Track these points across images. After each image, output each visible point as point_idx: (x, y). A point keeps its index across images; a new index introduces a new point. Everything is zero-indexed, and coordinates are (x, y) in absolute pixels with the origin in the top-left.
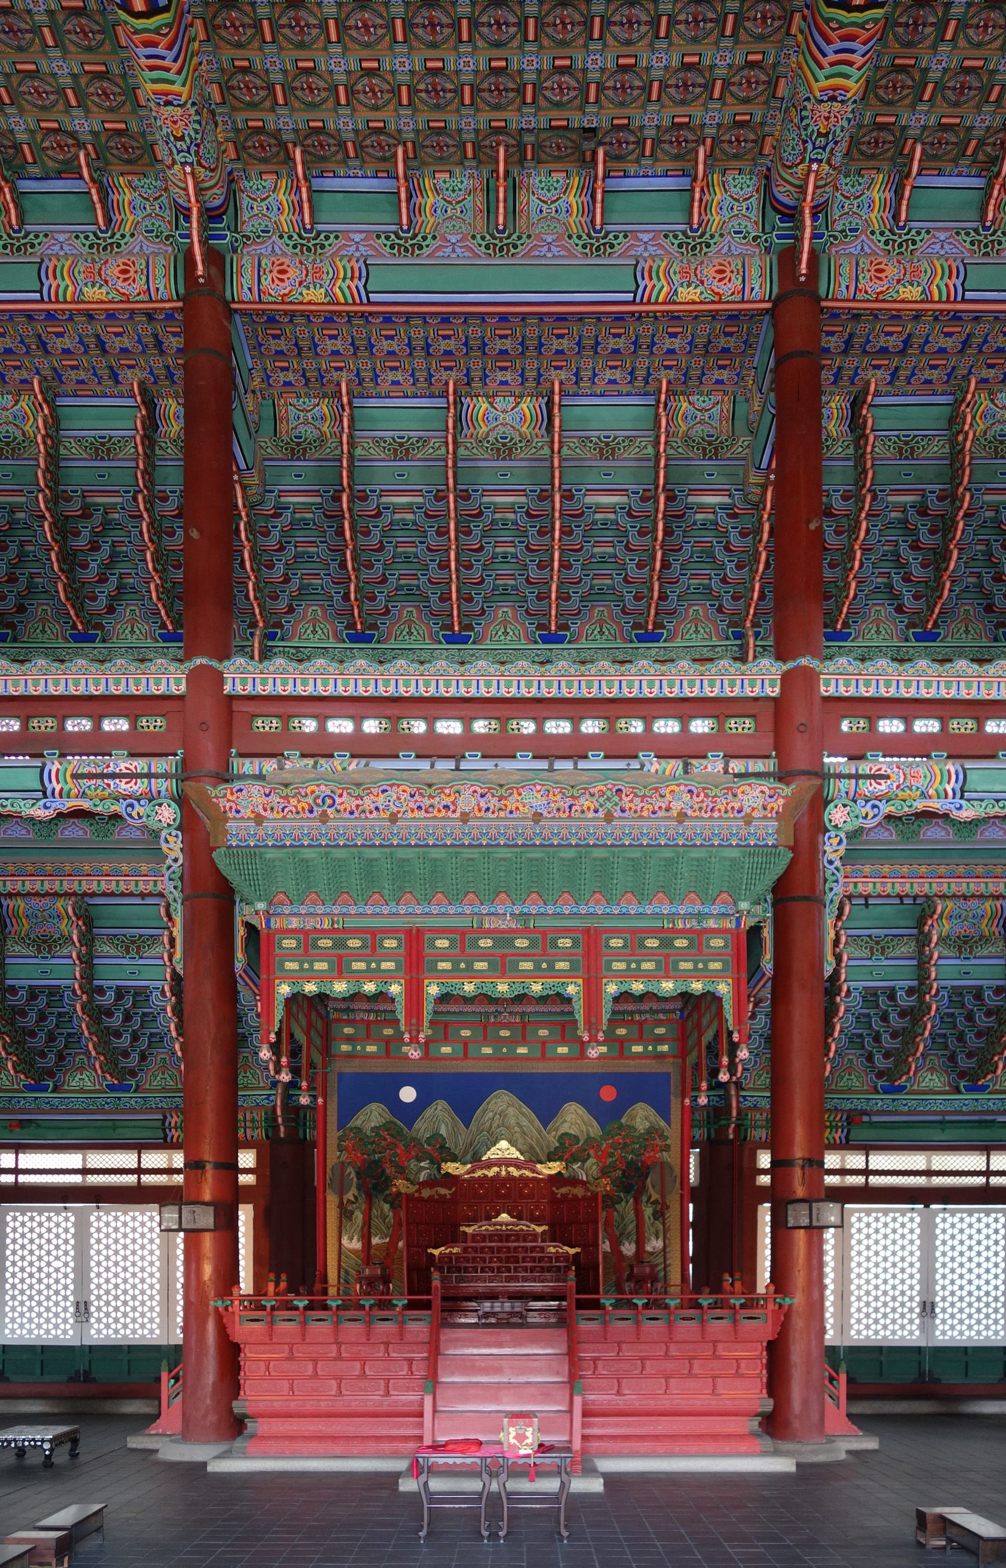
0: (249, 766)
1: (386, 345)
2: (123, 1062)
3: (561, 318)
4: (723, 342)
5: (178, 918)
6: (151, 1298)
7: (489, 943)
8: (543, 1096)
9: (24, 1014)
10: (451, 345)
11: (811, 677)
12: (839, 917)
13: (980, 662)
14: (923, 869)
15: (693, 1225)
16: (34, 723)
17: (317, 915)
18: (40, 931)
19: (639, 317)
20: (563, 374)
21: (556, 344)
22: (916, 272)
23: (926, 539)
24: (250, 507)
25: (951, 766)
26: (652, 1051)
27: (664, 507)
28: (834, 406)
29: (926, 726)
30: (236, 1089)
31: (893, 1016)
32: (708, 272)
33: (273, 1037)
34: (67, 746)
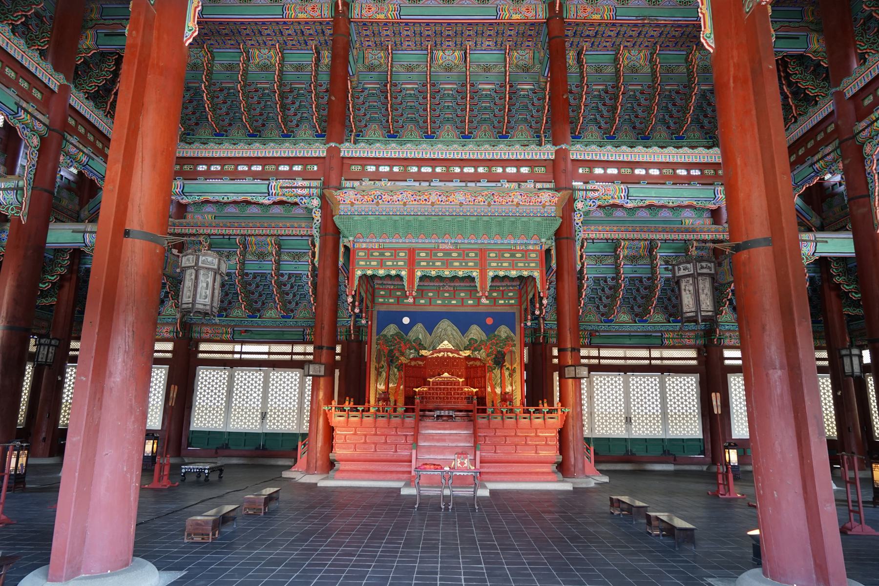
0: (348, 184)
1: (406, 33)
2: (289, 306)
3: (470, 24)
4: (529, 32)
5: (317, 244)
6: (294, 411)
7: (442, 254)
8: (463, 322)
9: (250, 285)
10: (430, 33)
11: (566, 151)
12: (582, 247)
13: (632, 147)
14: (615, 228)
19: (498, 24)
20: (470, 43)
21: (468, 33)
22: (598, 10)
23: (608, 101)
24: (353, 88)
25: (623, 186)
26: (508, 302)
27: (508, 91)
28: (571, 55)
30: (337, 318)
31: (606, 289)
32: (523, 9)
33: (353, 293)
34: (279, 176)
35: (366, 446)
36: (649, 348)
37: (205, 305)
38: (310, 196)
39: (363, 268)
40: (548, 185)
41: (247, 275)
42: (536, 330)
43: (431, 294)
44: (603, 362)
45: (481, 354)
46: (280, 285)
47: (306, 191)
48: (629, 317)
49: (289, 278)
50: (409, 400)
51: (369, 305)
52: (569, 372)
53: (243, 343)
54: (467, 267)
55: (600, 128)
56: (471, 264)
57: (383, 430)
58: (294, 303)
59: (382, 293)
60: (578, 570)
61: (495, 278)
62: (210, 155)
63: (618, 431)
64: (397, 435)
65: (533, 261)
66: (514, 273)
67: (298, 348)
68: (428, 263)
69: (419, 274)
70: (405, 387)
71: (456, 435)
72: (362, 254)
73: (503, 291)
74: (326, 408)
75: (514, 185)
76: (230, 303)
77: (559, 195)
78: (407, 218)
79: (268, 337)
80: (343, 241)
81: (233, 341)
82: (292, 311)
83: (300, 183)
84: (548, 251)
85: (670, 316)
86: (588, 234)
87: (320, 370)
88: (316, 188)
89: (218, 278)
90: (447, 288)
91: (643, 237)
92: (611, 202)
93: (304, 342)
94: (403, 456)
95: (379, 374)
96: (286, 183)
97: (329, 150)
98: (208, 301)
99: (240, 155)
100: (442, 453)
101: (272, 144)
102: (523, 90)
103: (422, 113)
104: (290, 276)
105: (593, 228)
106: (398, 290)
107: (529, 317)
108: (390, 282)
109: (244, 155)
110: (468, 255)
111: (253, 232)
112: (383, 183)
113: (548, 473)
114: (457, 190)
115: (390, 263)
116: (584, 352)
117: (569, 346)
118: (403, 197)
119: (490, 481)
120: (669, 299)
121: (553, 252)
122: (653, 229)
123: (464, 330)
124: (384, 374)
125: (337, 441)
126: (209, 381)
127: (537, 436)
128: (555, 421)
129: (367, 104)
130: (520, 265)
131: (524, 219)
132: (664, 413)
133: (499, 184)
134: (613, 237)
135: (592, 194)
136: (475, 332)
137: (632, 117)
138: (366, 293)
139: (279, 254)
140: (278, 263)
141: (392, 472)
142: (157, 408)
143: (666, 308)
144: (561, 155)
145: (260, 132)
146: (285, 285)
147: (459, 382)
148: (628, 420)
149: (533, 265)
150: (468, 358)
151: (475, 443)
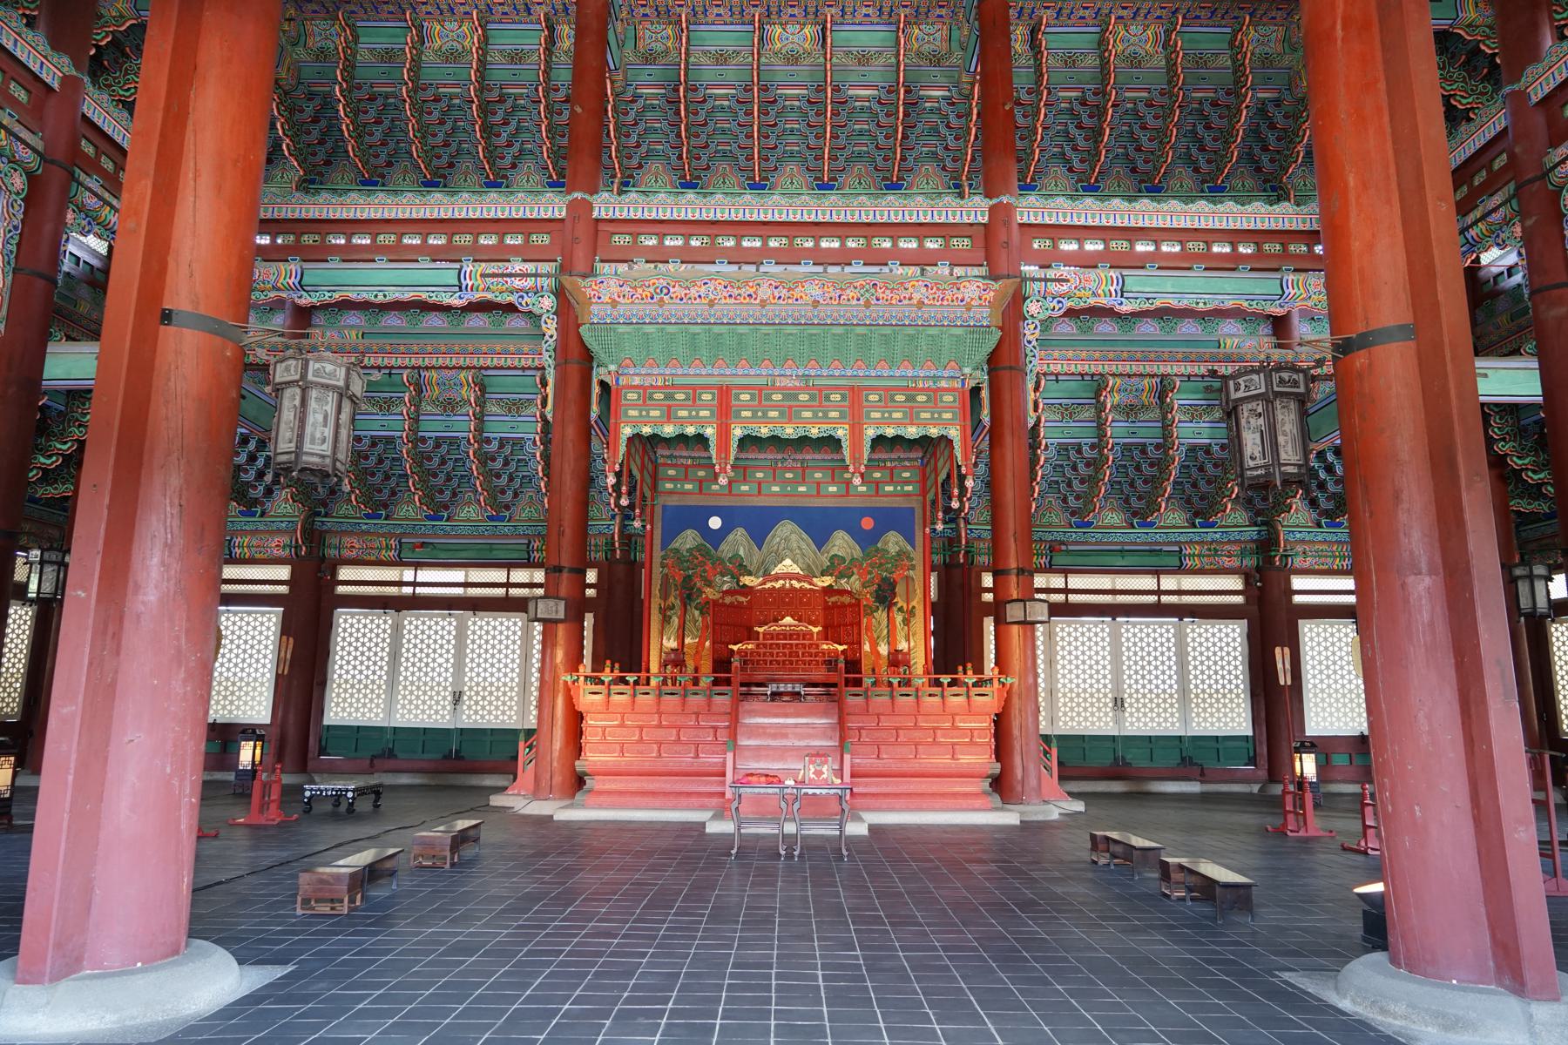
0: (607, 268)
2: (501, 498)
5: (551, 380)
7: (780, 397)
8: (818, 525)
9: (430, 459)
11: (1009, 209)
12: (1036, 389)
14: (1097, 355)
15: (933, 633)
16: (456, 238)
17: (655, 376)
18: (447, 395)
25: (1114, 273)
26: (901, 489)
29: (1093, 246)
31: (1081, 466)
35: (641, 747)
36: (1157, 573)
37: (323, 457)
38: (536, 291)
39: (635, 423)
40: (976, 271)
41: (424, 440)
42: (952, 542)
43: (760, 475)
44: (1073, 598)
45: (853, 583)
46: (485, 459)
47: (530, 282)
48: (1122, 516)
49: (501, 446)
50: (722, 664)
51: (648, 494)
52: (1014, 612)
53: (417, 566)
54: (826, 419)
55: (1071, 170)
56: (833, 414)
57: (673, 718)
58: (510, 494)
59: (671, 472)
60: (1035, 959)
61: (879, 441)
62: (351, 216)
63: (1100, 723)
64: (698, 727)
65: (948, 408)
66: (912, 432)
67: (519, 576)
68: (755, 413)
69: (737, 432)
70: (713, 643)
71: (806, 726)
72: (632, 396)
73: (892, 469)
74: (568, 678)
75: (910, 270)
76: (393, 493)
77: (996, 286)
78: (716, 329)
79: (464, 554)
80: (599, 374)
81: (399, 563)
82: (507, 508)
83: (518, 266)
84: (976, 391)
85: (1196, 515)
86: (1048, 363)
87: (557, 609)
88: (548, 275)
89: (347, 407)
90: (789, 463)
91: (1148, 370)
92: (1092, 301)
93: (529, 564)
94: (710, 764)
95: (666, 620)
96: (492, 268)
97: (571, 206)
98: (326, 448)
99: (407, 216)
100: (782, 758)
101: (465, 195)
102: (930, 98)
103: (743, 141)
104: (502, 443)
105: (1056, 354)
106: (700, 466)
107: (940, 514)
108: (685, 453)
109: (414, 216)
110: (827, 398)
111: (434, 362)
112: (671, 266)
113: (976, 795)
114: (810, 277)
115: (684, 413)
116: (1040, 581)
117: (1013, 564)
118: (710, 290)
119: (869, 809)
120: (1194, 485)
121: (985, 394)
122: (1166, 356)
123: (821, 540)
124: (675, 621)
125: (590, 738)
126: (356, 637)
127: (954, 727)
128: (989, 701)
129: (642, 126)
130: (923, 415)
131: (931, 331)
132: (1184, 692)
133: (886, 269)
134: (1093, 370)
135: (1056, 286)
136: (842, 543)
137: (1131, 149)
138: (641, 472)
139: (481, 402)
140: (480, 419)
141: (689, 794)
142: (262, 684)
143: (1188, 501)
144: (1000, 214)
145: (444, 177)
146: (493, 460)
147: (811, 634)
148: (1119, 703)
149: (947, 416)
150: (828, 591)
151: (842, 739)
